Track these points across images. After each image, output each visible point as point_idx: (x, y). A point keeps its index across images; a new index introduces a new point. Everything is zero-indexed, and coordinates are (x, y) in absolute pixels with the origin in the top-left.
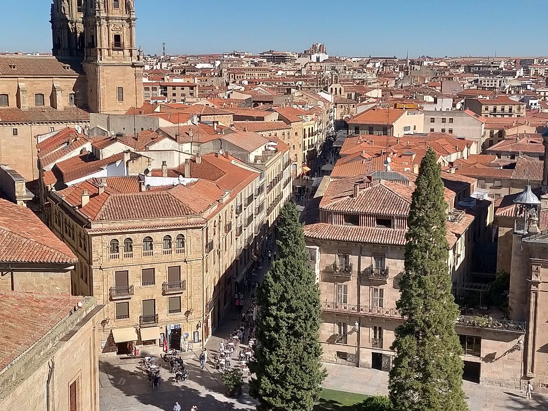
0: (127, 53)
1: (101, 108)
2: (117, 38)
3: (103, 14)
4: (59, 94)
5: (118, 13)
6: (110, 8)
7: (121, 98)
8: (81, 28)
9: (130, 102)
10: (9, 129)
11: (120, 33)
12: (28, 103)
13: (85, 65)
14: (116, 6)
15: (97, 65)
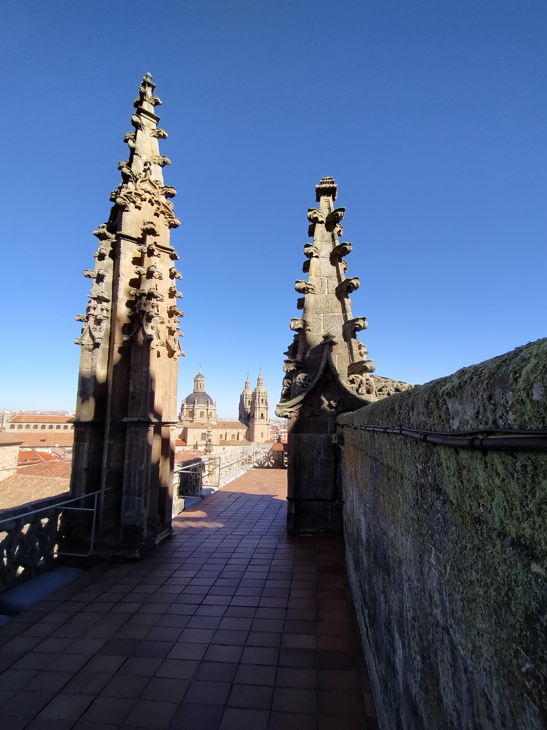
0: (265, 420)
1: (255, 441)
2: (262, 415)
3: (258, 406)
4: (240, 435)
5: (263, 406)
6: (260, 404)
7: (262, 437)
8: (249, 411)
9: (265, 438)
10: (222, 447)
11: (263, 413)
12: (229, 438)
13: (250, 424)
14: (262, 403)
15: (254, 424)
